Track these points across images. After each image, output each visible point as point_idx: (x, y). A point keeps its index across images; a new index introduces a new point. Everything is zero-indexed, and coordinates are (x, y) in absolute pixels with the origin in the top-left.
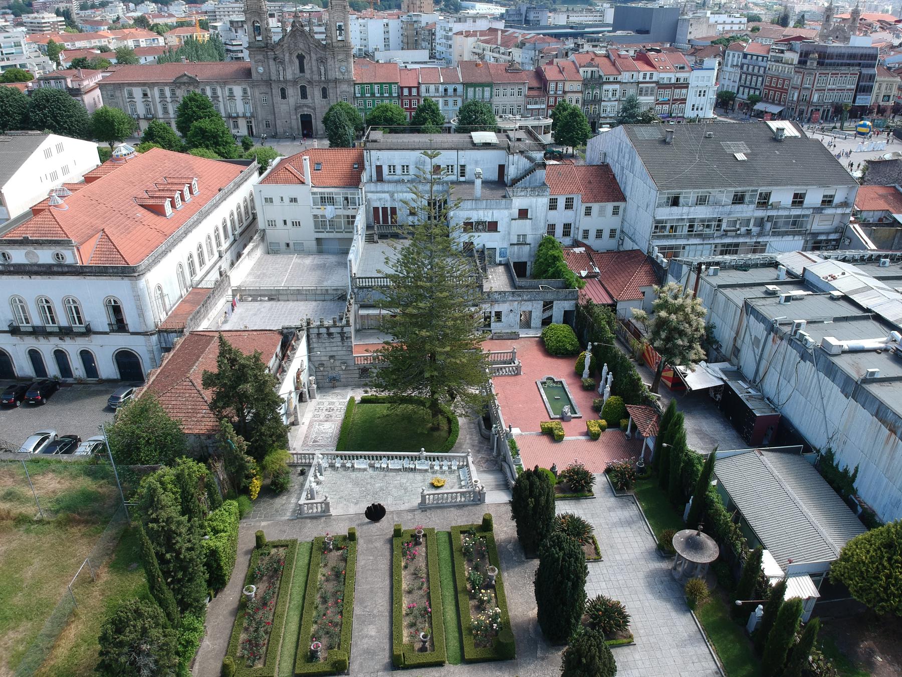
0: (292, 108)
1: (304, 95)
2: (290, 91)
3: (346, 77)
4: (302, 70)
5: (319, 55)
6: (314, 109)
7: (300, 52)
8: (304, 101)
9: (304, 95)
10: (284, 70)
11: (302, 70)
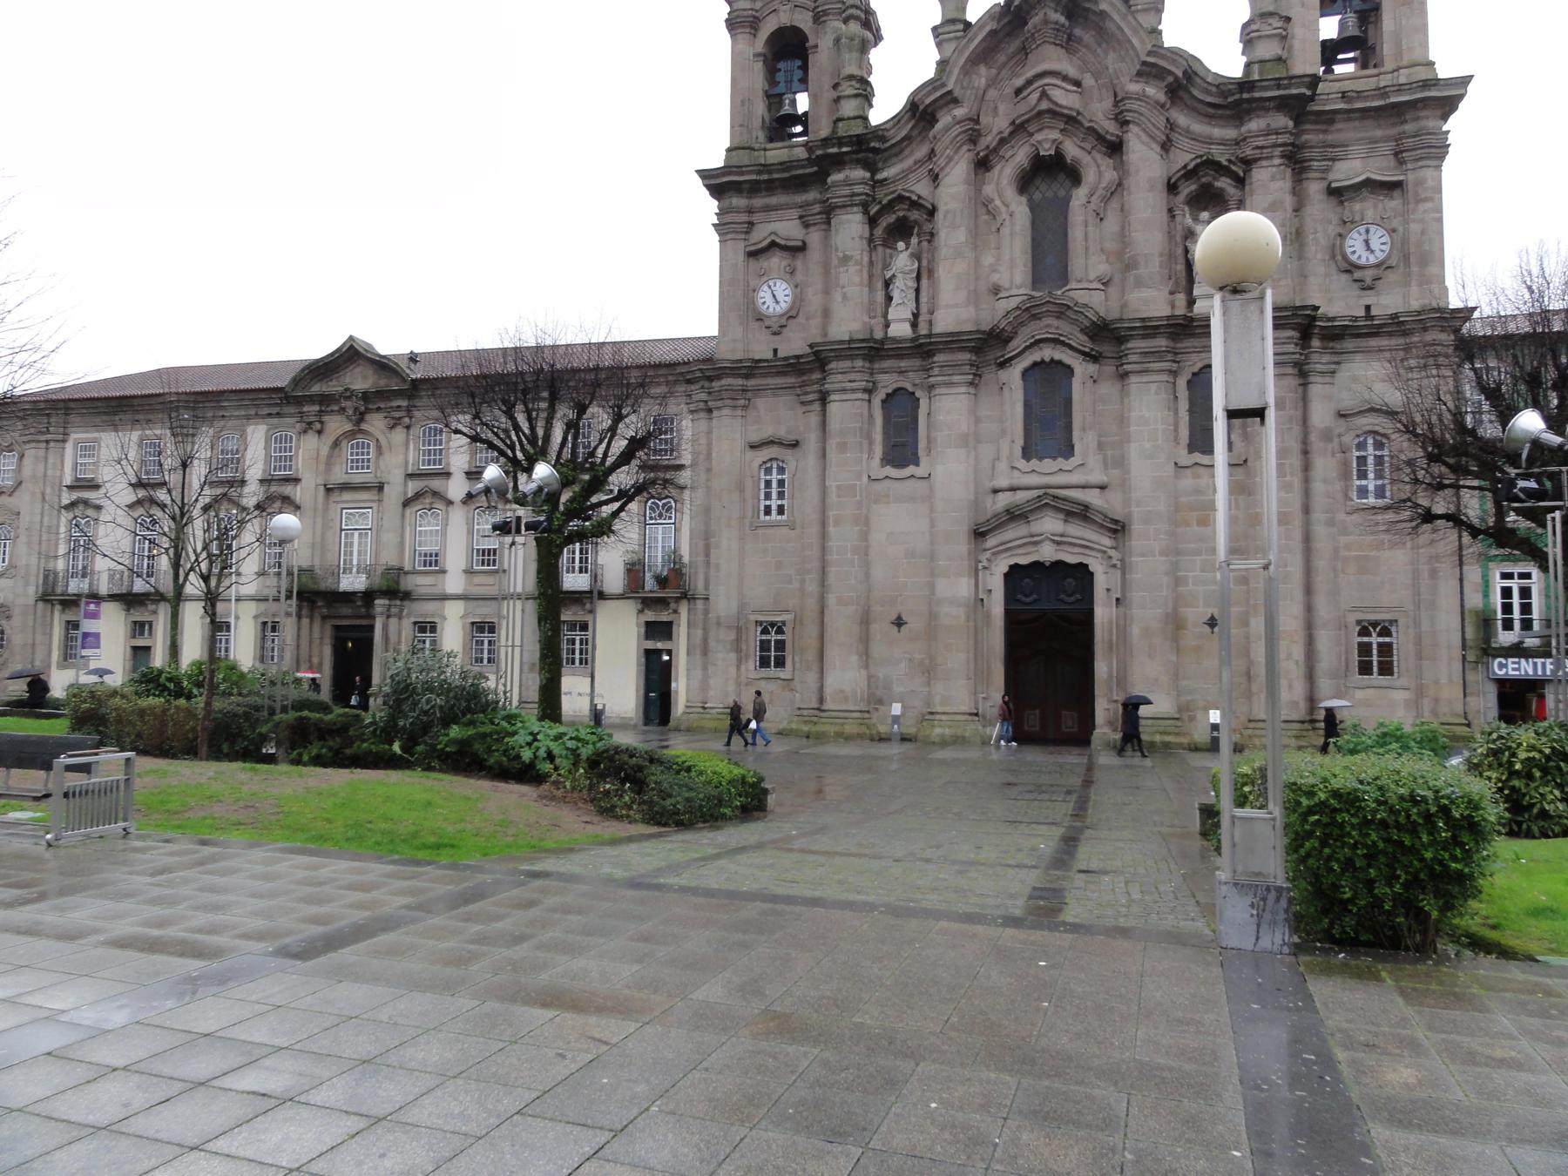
0: (957, 525)
1: (1048, 429)
2: (949, 410)
3: (1387, 302)
4: (1050, 254)
5: (1183, 157)
6: (1118, 529)
7: (1047, 139)
8: (1047, 472)
9: (1048, 429)
10: (923, 274)
11: (1050, 254)
